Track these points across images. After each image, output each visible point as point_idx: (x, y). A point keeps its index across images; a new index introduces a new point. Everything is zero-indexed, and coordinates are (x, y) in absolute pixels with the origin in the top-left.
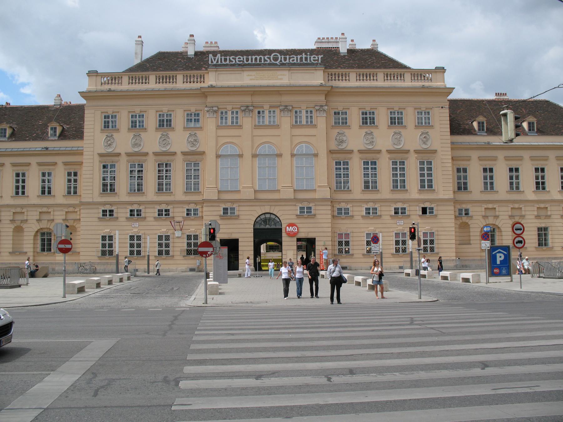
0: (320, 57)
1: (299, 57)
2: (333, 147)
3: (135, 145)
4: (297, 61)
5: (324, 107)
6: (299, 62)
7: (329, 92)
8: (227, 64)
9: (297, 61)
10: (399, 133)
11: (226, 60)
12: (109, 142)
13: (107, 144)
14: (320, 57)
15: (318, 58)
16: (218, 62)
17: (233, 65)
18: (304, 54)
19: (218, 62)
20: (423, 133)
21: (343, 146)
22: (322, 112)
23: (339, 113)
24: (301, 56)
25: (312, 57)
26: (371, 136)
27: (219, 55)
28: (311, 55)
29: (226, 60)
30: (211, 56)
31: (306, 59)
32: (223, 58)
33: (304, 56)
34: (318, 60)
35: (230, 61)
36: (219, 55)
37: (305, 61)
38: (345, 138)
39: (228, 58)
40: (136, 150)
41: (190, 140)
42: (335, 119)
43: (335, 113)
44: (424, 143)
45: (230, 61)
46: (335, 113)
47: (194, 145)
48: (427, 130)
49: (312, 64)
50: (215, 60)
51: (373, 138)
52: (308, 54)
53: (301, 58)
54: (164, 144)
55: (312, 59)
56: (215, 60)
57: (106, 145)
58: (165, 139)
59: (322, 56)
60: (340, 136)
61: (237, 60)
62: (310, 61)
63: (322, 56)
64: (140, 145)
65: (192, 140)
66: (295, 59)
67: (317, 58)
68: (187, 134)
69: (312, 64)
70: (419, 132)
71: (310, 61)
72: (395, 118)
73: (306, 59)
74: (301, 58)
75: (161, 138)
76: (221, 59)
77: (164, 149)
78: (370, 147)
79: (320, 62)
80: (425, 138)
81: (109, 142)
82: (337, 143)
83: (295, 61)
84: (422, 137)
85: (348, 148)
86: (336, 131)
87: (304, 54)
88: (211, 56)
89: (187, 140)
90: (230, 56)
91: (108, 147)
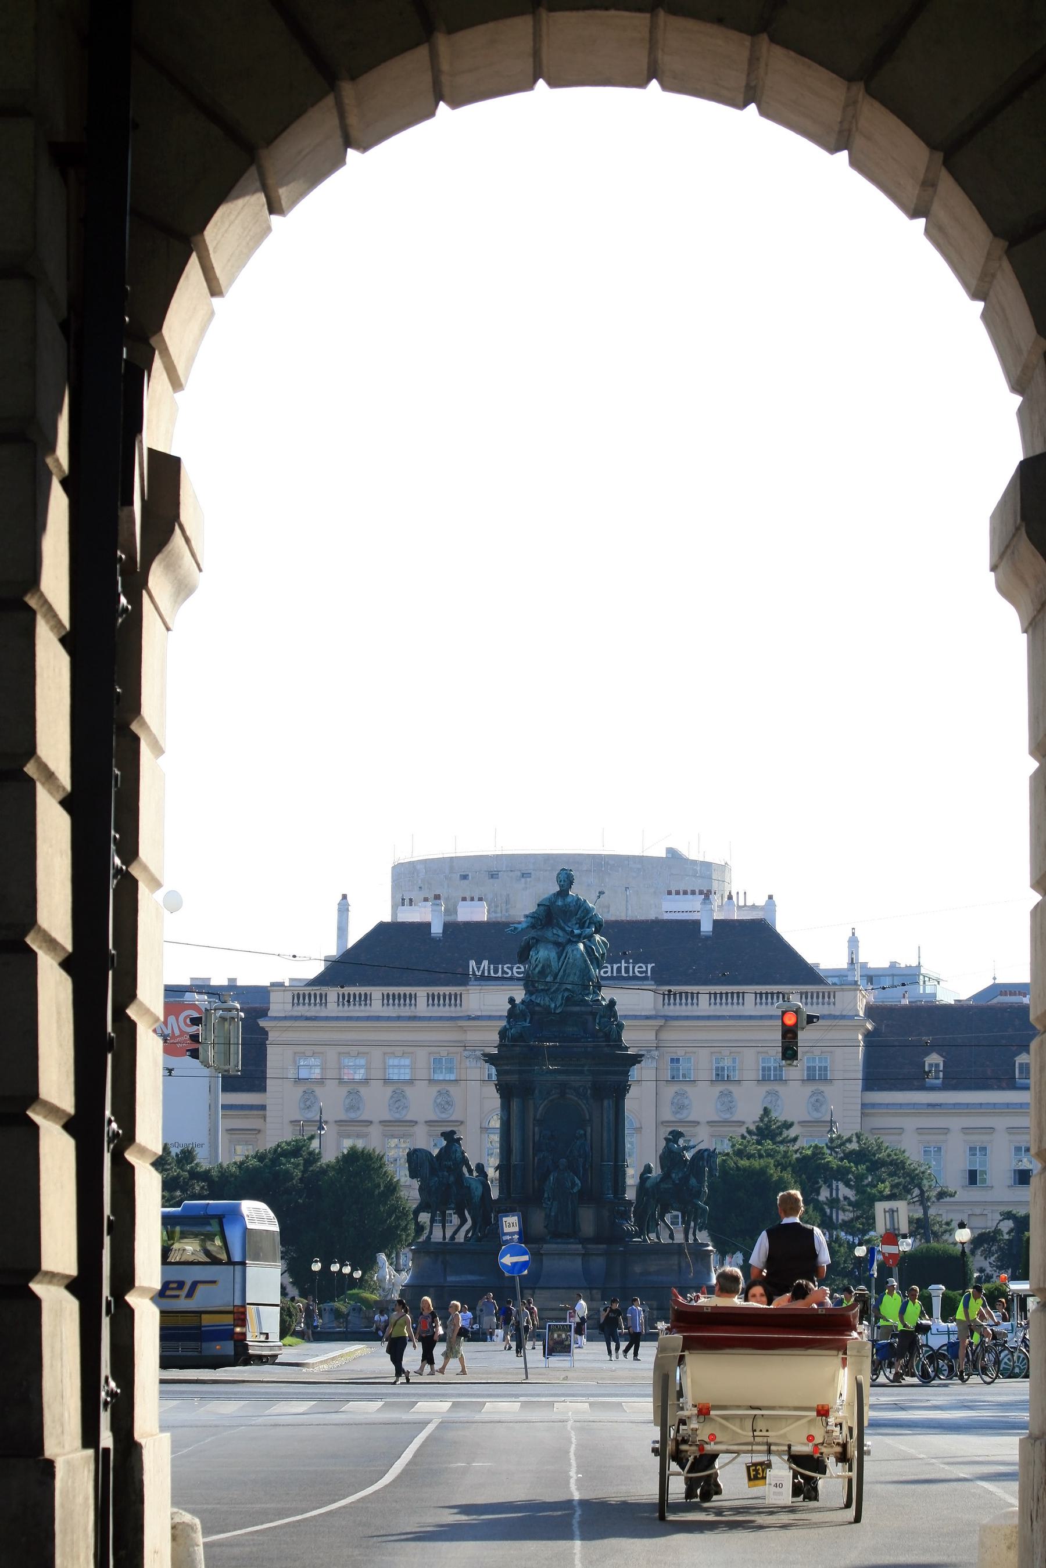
0: (650, 966)
1: (615, 966)
2: (667, 1115)
3: (351, 1108)
4: (612, 972)
5: (653, 1052)
6: (615, 974)
7: (661, 1026)
8: (498, 977)
9: (612, 972)
10: (776, 1093)
11: (496, 971)
12: (308, 1103)
13: (306, 1105)
14: (650, 966)
15: (647, 967)
16: (483, 972)
17: (511, 979)
18: (623, 961)
19: (483, 972)
20: (814, 1094)
21: (683, 1116)
22: (650, 1060)
23: (678, 1060)
24: (619, 965)
25: (638, 965)
26: (729, 1099)
27: (485, 963)
28: (635, 963)
29: (496, 971)
30: (472, 963)
31: (627, 970)
32: (492, 967)
33: (624, 965)
34: (646, 972)
35: (504, 972)
36: (485, 963)
37: (625, 973)
38: (686, 1102)
39: (500, 966)
40: (352, 1116)
41: (439, 1101)
42: (672, 1069)
43: (672, 1060)
44: (817, 1110)
45: (504, 972)
46: (672, 1060)
47: (444, 1110)
48: (822, 1088)
49: (635, 978)
50: (478, 969)
51: (731, 1102)
52: (631, 961)
53: (619, 969)
54: (397, 1108)
55: (636, 970)
56: (478, 969)
57: (302, 1106)
58: (399, 1100)
59: (654, 965)
60: (679, 1097)
61: (515, 970)
62: (634, 972)
63: (654, 965)
64: (358, 1109)
65: (443, 1103)
66: (609, 969)
67: (644, 969)
68: (434, 1090)
69: (635, 978)
70: (810, 1088)
71: (634, 972)
72: (769, 1069)
73: (627, 970)
74: (619, 969)
75: (392, 1097)
76: (489, 967)
77: (397, 1116)
78: (727, 1116)
79: (649, 974)
80: (818, 1101)
81: (308, 1103)
82: (674, 1110)
83: (609, 974)
84: (814, 1098)
85: (691, 1118)
86: (673, 1089)
87: (623, 961)
88: (472, 963)
89: (435, 1101)
90: (503, 964)
91: (307, 1111)
